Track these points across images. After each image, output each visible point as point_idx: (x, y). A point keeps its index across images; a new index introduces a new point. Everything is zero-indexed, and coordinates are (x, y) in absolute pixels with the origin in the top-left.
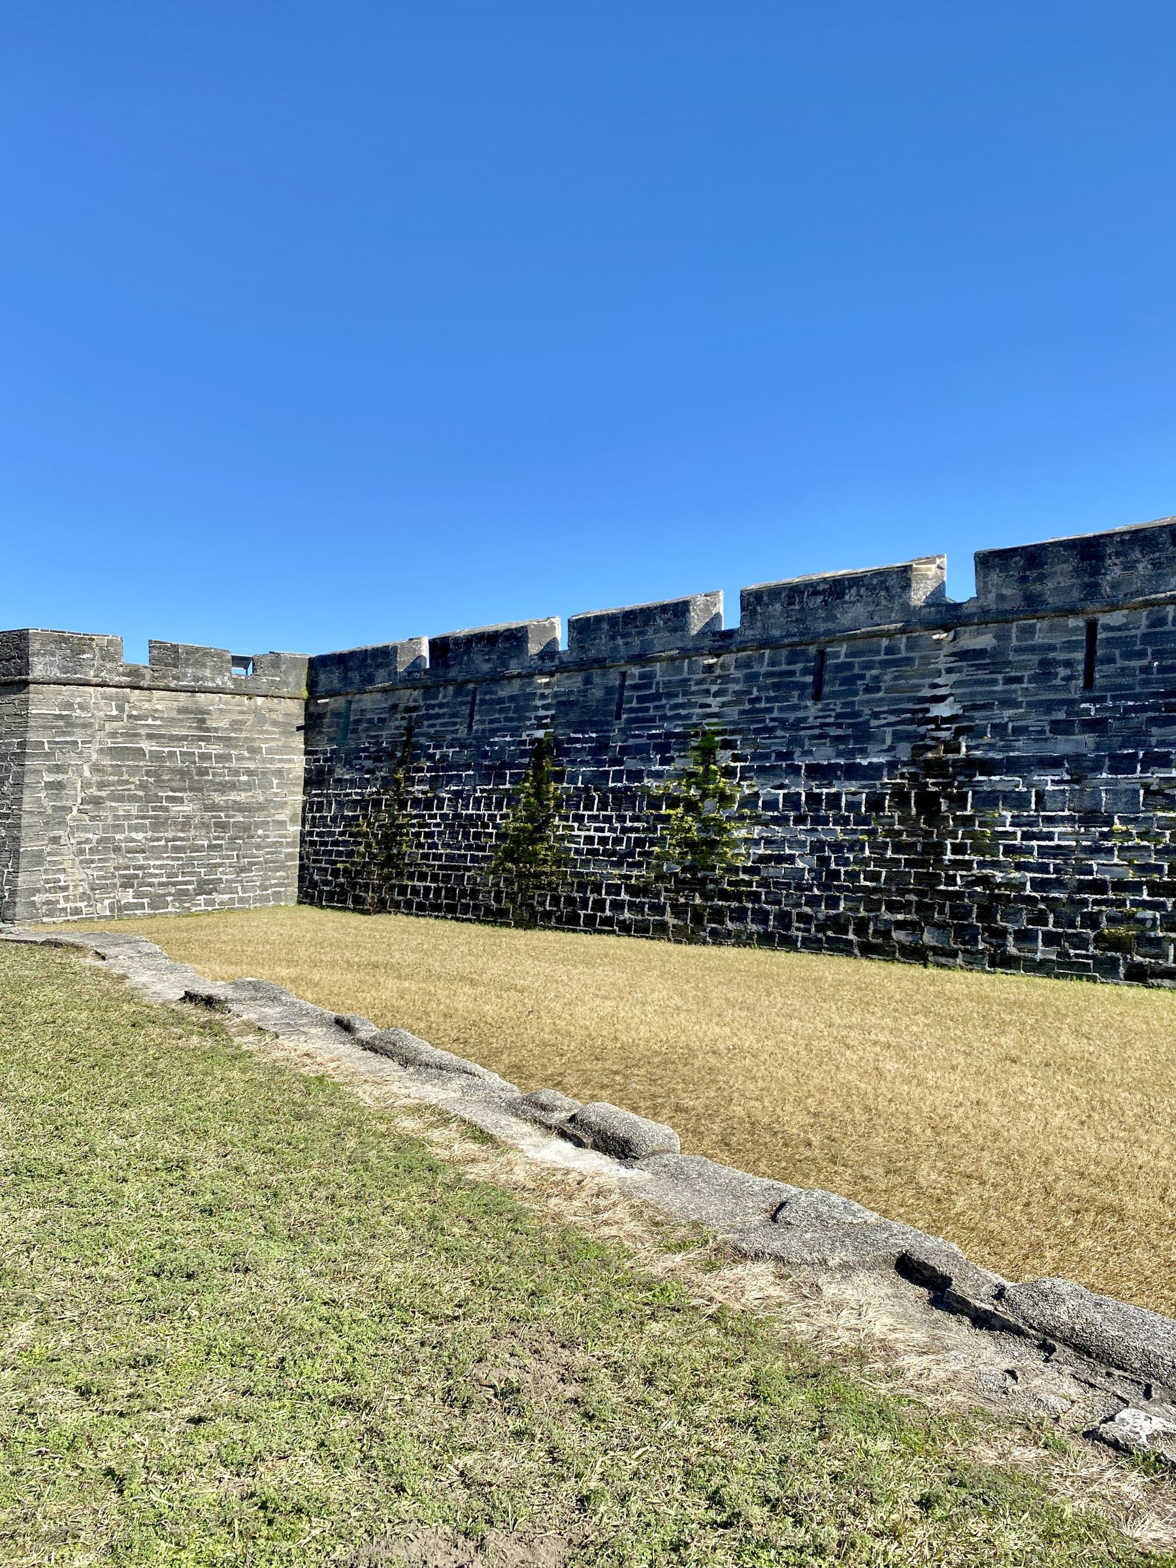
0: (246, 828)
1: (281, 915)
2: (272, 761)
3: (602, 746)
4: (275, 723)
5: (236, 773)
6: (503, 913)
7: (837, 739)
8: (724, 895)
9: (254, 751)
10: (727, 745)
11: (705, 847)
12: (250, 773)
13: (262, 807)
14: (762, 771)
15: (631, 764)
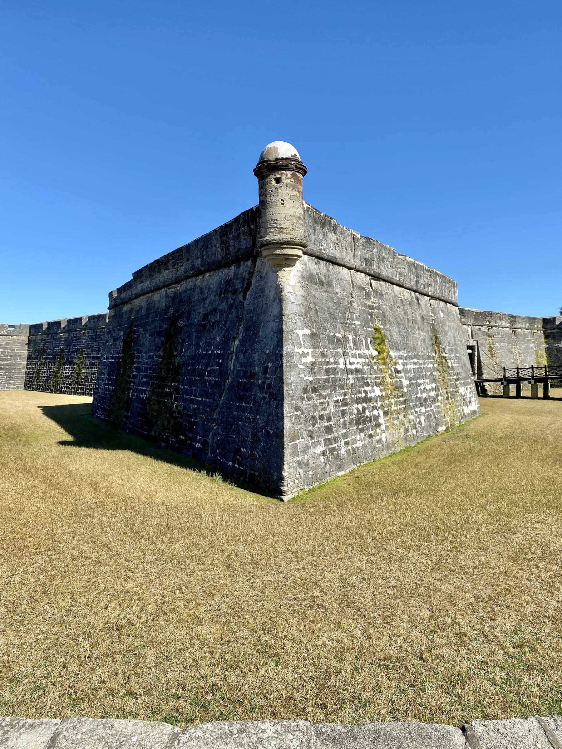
0: (9, 370)
1: (20, 392)
2: (18, 353)
3: (69, 352)
4: (19, 343)
5: (7, 356)
6: (52, 390)
7: (97, 351)
8: (80, 385)
9: (12, 350)
10: (84, 351)
11: (79, 374)
12: (11, 356)
13: (14, 365)
14: (88, 357)
15: (73, 355)
